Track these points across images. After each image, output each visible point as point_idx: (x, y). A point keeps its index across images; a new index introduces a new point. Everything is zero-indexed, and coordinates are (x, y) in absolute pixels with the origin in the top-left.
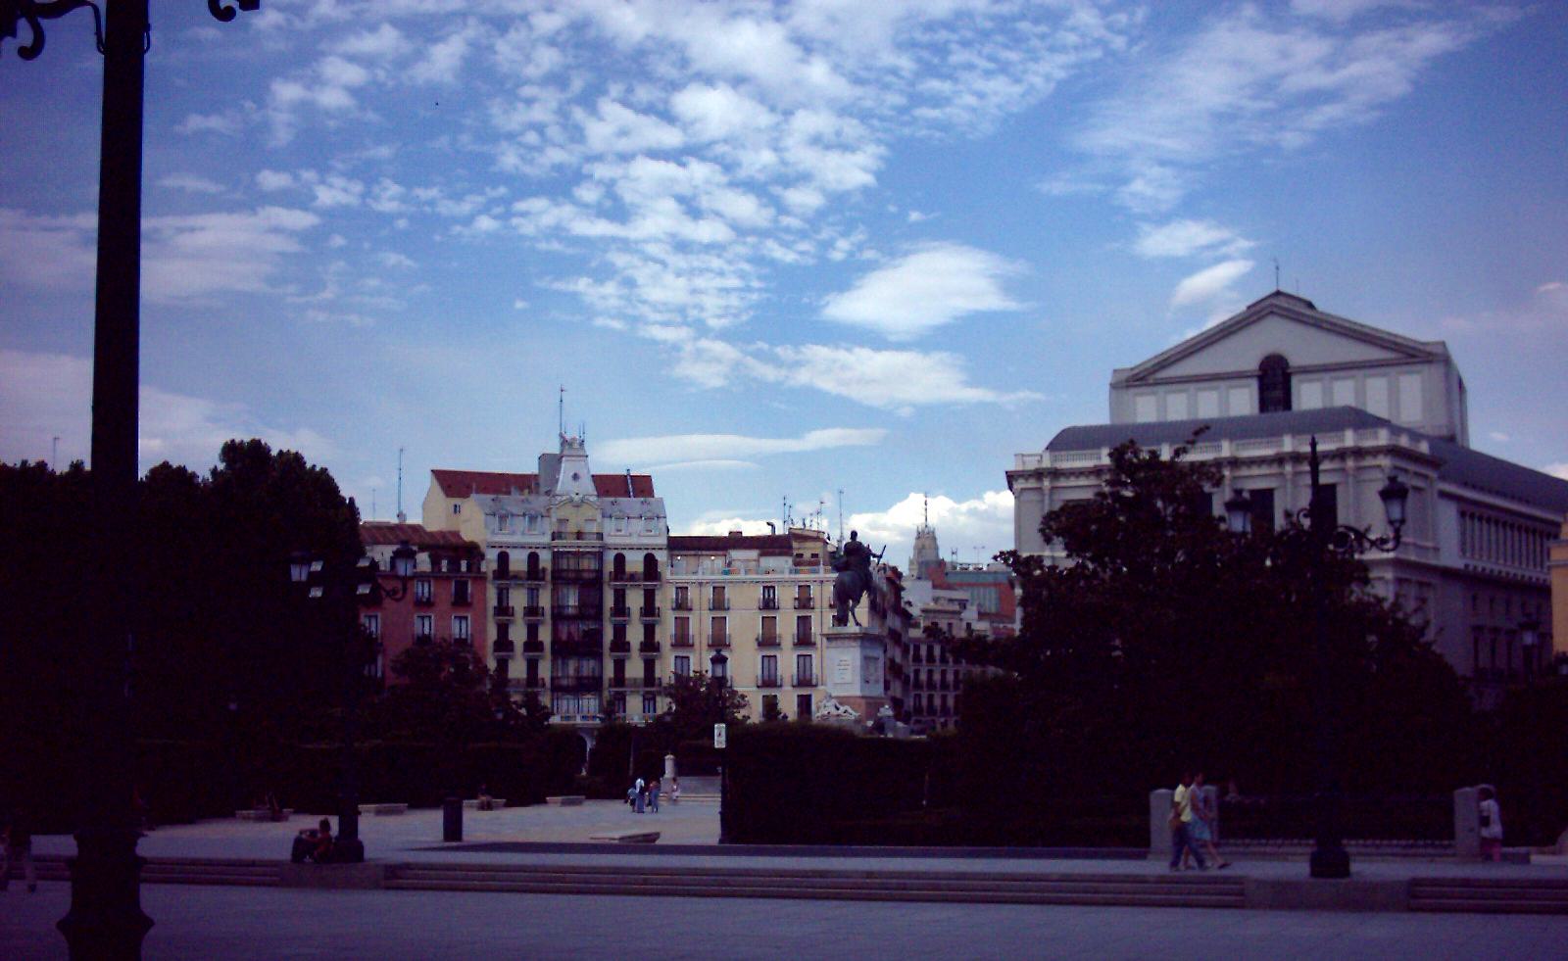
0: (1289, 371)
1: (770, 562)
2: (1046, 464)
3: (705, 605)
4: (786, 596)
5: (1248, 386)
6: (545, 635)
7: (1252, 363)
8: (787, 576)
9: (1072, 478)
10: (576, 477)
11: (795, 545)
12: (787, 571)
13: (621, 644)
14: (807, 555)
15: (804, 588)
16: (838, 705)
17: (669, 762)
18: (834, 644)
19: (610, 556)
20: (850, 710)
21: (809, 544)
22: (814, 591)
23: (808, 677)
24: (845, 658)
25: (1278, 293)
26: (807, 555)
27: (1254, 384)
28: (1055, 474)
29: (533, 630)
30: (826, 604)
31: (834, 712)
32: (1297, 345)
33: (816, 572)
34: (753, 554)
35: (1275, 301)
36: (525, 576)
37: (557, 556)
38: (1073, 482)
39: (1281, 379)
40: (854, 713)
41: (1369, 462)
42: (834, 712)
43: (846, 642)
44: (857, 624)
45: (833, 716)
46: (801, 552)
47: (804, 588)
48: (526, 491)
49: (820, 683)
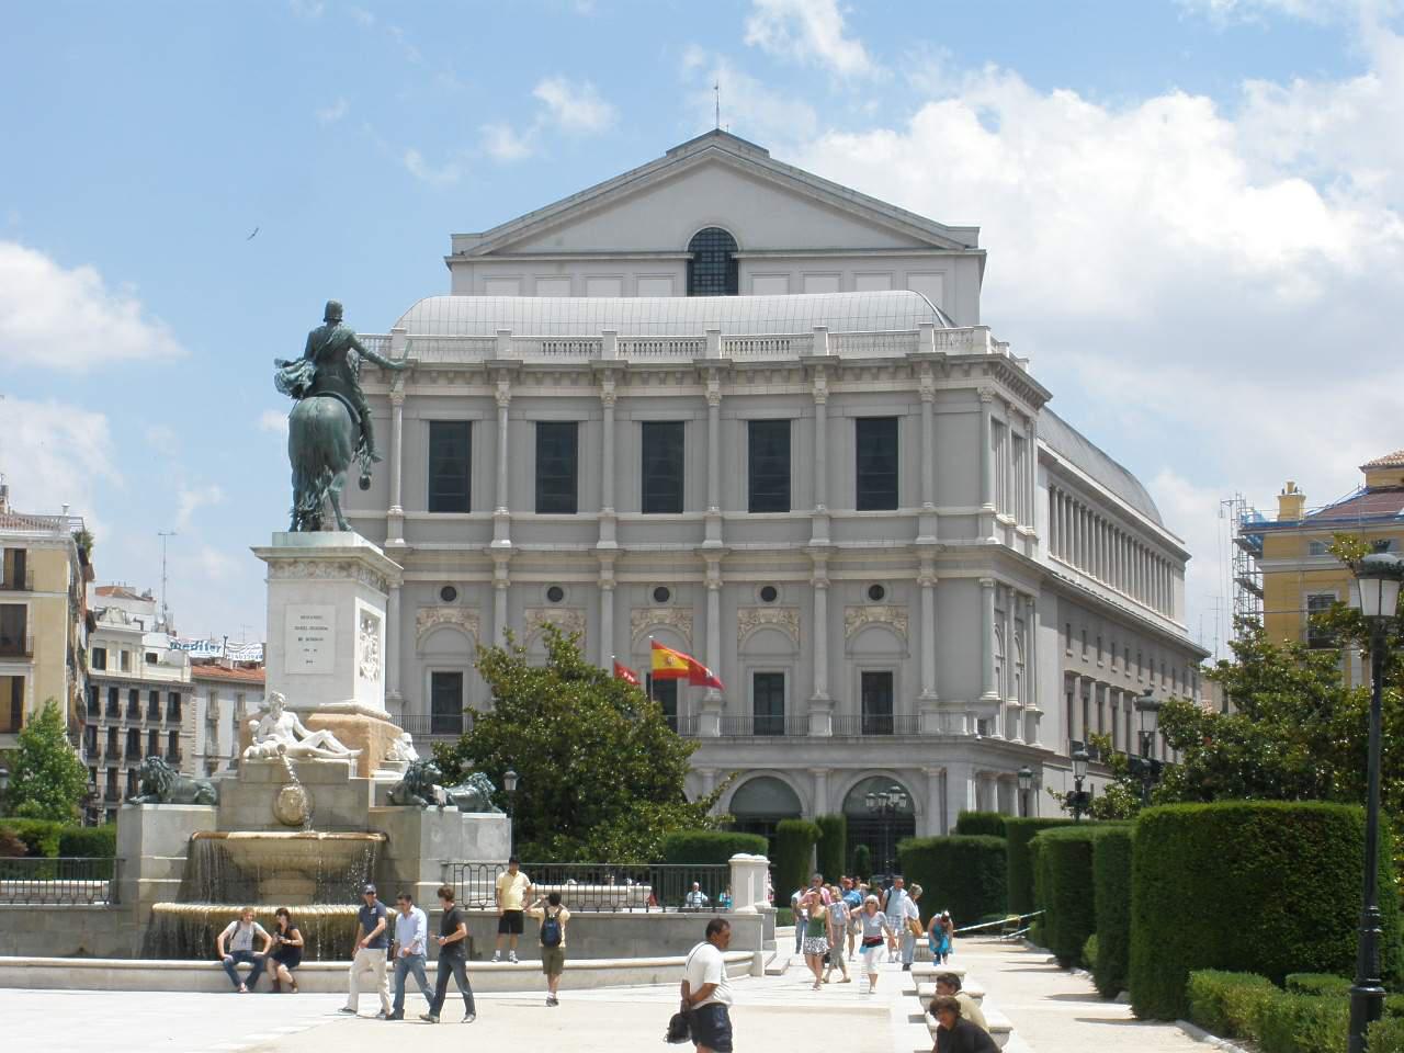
0: (736, 256)
5: (670, 276)
9: (442, 381)
20: (333, 742)
24: (318, 610)
25: (717, 132)
31: (292, 744)
32: (752, 220)
38: (441, 389)
39: (719, 268)
40: (345, 751)
41: (956, 382)
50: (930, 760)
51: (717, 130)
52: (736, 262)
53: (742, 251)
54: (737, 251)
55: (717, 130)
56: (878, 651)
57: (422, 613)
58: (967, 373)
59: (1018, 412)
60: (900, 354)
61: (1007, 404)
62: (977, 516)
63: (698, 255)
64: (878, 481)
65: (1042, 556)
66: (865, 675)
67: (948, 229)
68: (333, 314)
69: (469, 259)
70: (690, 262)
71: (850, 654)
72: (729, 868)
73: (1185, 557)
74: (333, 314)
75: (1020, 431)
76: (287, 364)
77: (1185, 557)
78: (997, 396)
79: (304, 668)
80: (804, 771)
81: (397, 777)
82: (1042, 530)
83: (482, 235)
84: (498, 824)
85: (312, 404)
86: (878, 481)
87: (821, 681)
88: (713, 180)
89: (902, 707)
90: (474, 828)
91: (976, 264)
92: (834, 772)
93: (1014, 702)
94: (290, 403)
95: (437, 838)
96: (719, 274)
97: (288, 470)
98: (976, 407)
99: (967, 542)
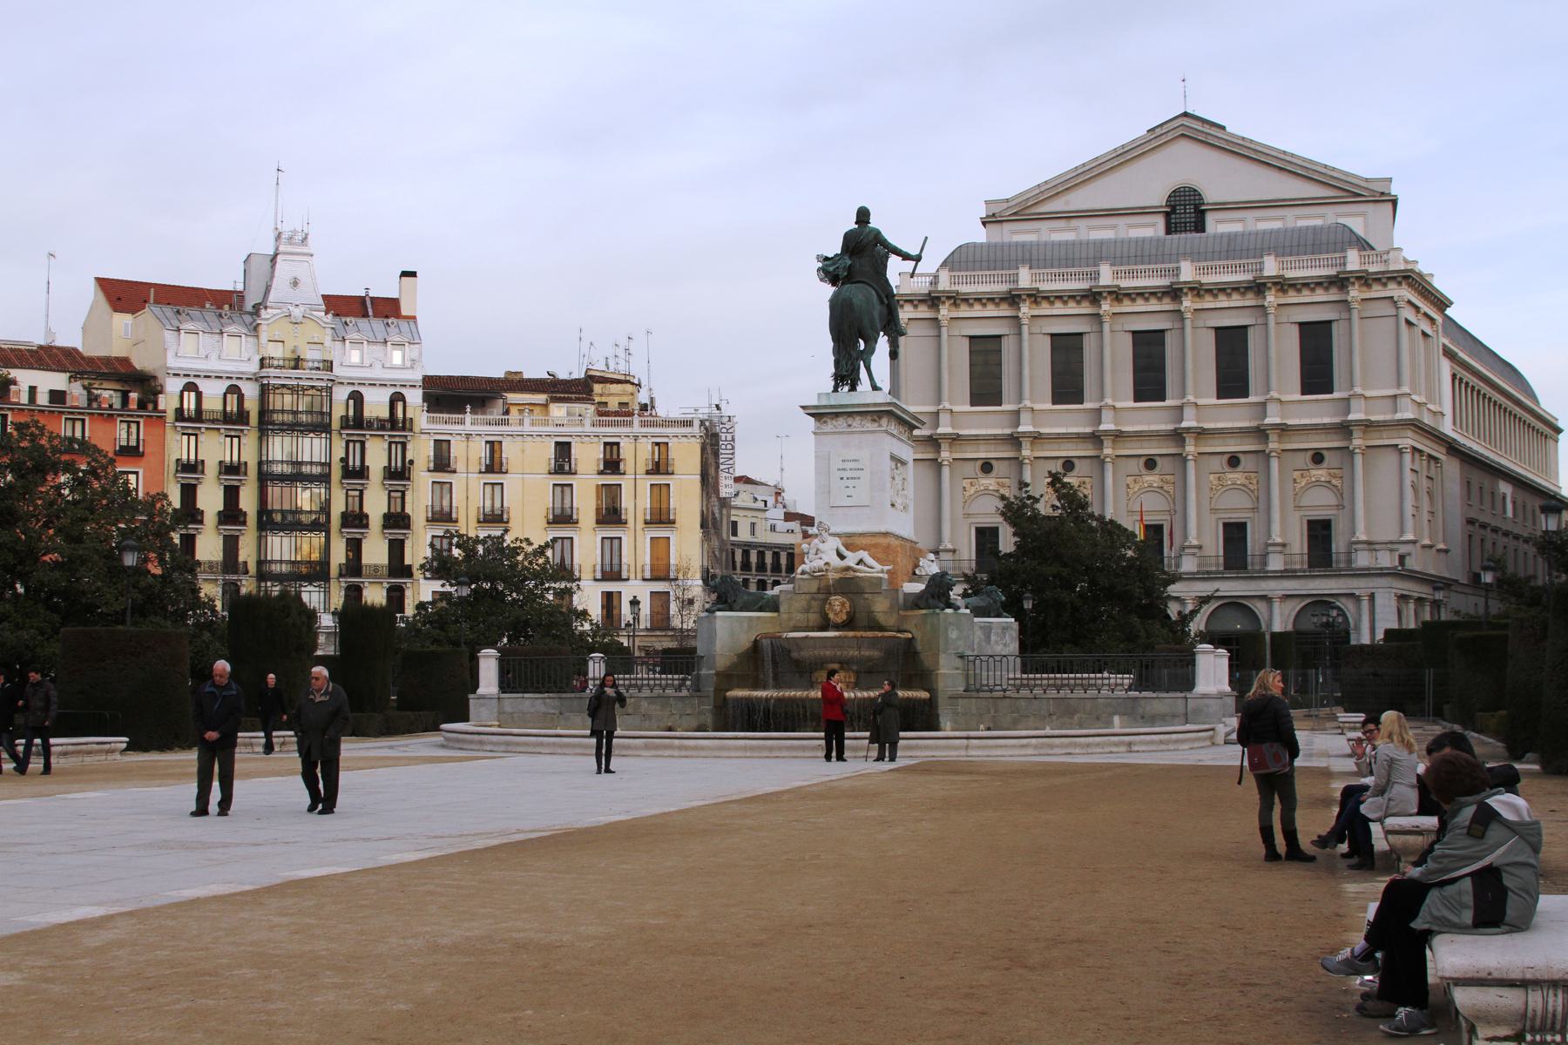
1: (558, 411)
2: (944, 284)
3: (474, 467)
4: (588, 456)
6: (248, 501)
7: (1158, 198)
8: (588, 428)
10: (295, 283)
11: (597, 388)
12: (588, 422)
13: (356, 519)
14: (613, 404)
15: (611, 447)
16: (843, 549)
17: (488, 666)
18: (830, 426)
19: (341, 394)
21: (615, 388)
22: (626, 450)
23: (616, 568)
25: (1185, 114)
26: (613, 404)
27: (1160, 221)
28: (956, 299)
29: (231, 494)
30: (642, 469)
31: (836, 562)
32: (1217, 180)
33: (631, 424)
34: (541, 398)
35: (1186, 121)
36: (219, 417)
37: (265, 391)
39: (1190, 218)
40: (878, 567)
41: (1377, 291)
42: (836, 562)
43: (857, 422)
44: (875, 388)
45: (837, 570)
46: (604, 399)
47: (611, 447)
48: (226, 307)
49: (632, 576)
50: (1359, 586)
52: (1203, 212)
56: (1320, 503)
57: (966, 483)
59: (1425, 314)
60: (1332, 272)
61: (1417, 308)
62: (1395, 396)
63: (1173, 208)
64: (1317, 374)
65: (1447, 428)
66: (1309, 522)
67: (1367, 180)
68: (863, 216)
70: (1167, 214)
71: (1298, 508)
72: (1194, 654)
73: (1558, 431)
74: (863, 216)
75: (1429, 331)
76: (827, 259)
77: (1558, 431)
78: (1409, 302)
79: (848, 502)
80: (1263, 598)
81: (918, 587)
82: (1447, 408)
84: (1005, 628)
85: (851, 290)
86: (1317, 374)
87: (1276, 527)
88: (1185, 147)
89: (1338, 545)
90: (987, 630)
91: (1390, 205)
92: (1287, 597)
93: (1427, 542)
94: (829, 290)
95: (953, 634)
97: (828, 343)
98: (1392, 311)
99: (1388, 417)
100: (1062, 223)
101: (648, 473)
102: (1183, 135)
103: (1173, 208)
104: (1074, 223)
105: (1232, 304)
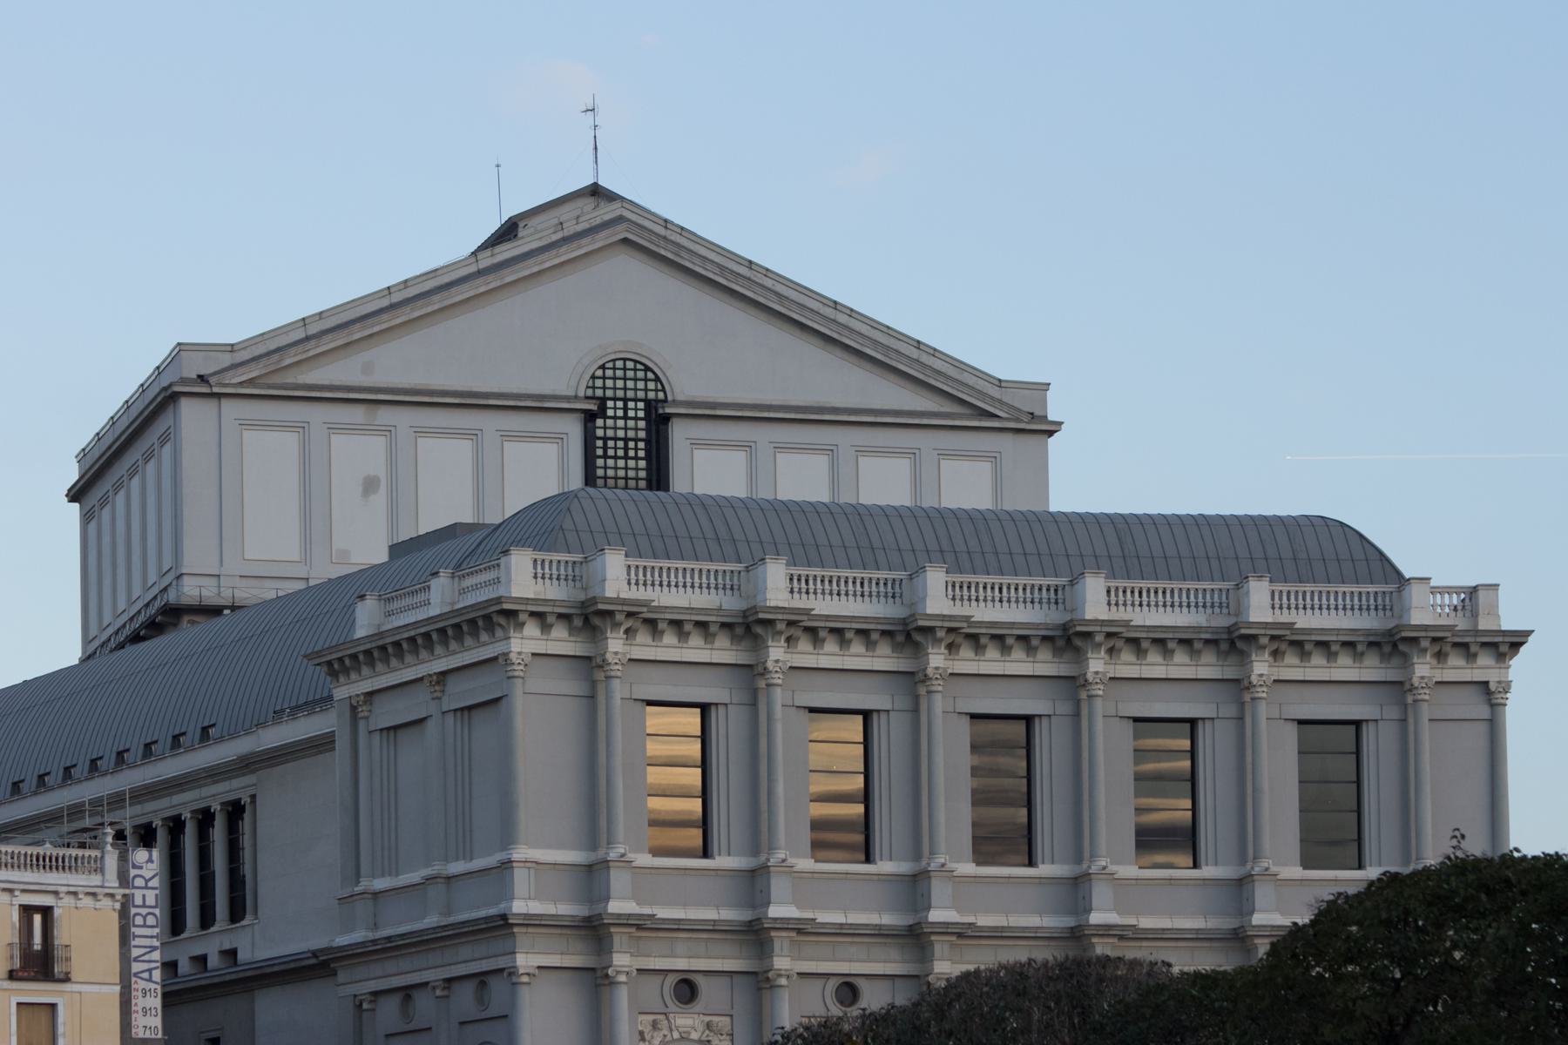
5: (559, 438)
7: (564, 375)
25: (595, 192)
27: (573, 429)
41: (1456, 669)
51: (595, 184)
52: (666, 419)
53: (675, 403)
54: (665, 401)
55: (595, 184)
58: (1471, 657)
69: (216, 390)
70: (589, 417)
83: (232, 348)
88: (629, 267)
96: (636, 440)
98: (1483, 711)
100: (357, 414)
101: (12, 976)
102: (625, 241)
103: (602, 412)
104: (385, 416)
105: (1175, 672)
